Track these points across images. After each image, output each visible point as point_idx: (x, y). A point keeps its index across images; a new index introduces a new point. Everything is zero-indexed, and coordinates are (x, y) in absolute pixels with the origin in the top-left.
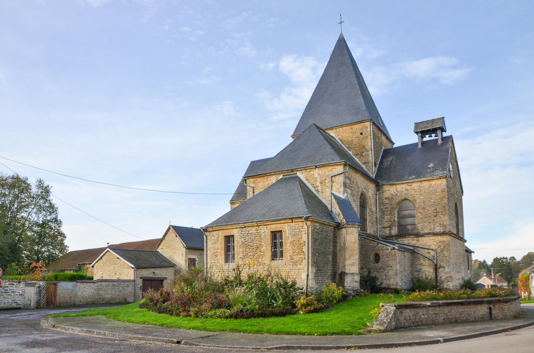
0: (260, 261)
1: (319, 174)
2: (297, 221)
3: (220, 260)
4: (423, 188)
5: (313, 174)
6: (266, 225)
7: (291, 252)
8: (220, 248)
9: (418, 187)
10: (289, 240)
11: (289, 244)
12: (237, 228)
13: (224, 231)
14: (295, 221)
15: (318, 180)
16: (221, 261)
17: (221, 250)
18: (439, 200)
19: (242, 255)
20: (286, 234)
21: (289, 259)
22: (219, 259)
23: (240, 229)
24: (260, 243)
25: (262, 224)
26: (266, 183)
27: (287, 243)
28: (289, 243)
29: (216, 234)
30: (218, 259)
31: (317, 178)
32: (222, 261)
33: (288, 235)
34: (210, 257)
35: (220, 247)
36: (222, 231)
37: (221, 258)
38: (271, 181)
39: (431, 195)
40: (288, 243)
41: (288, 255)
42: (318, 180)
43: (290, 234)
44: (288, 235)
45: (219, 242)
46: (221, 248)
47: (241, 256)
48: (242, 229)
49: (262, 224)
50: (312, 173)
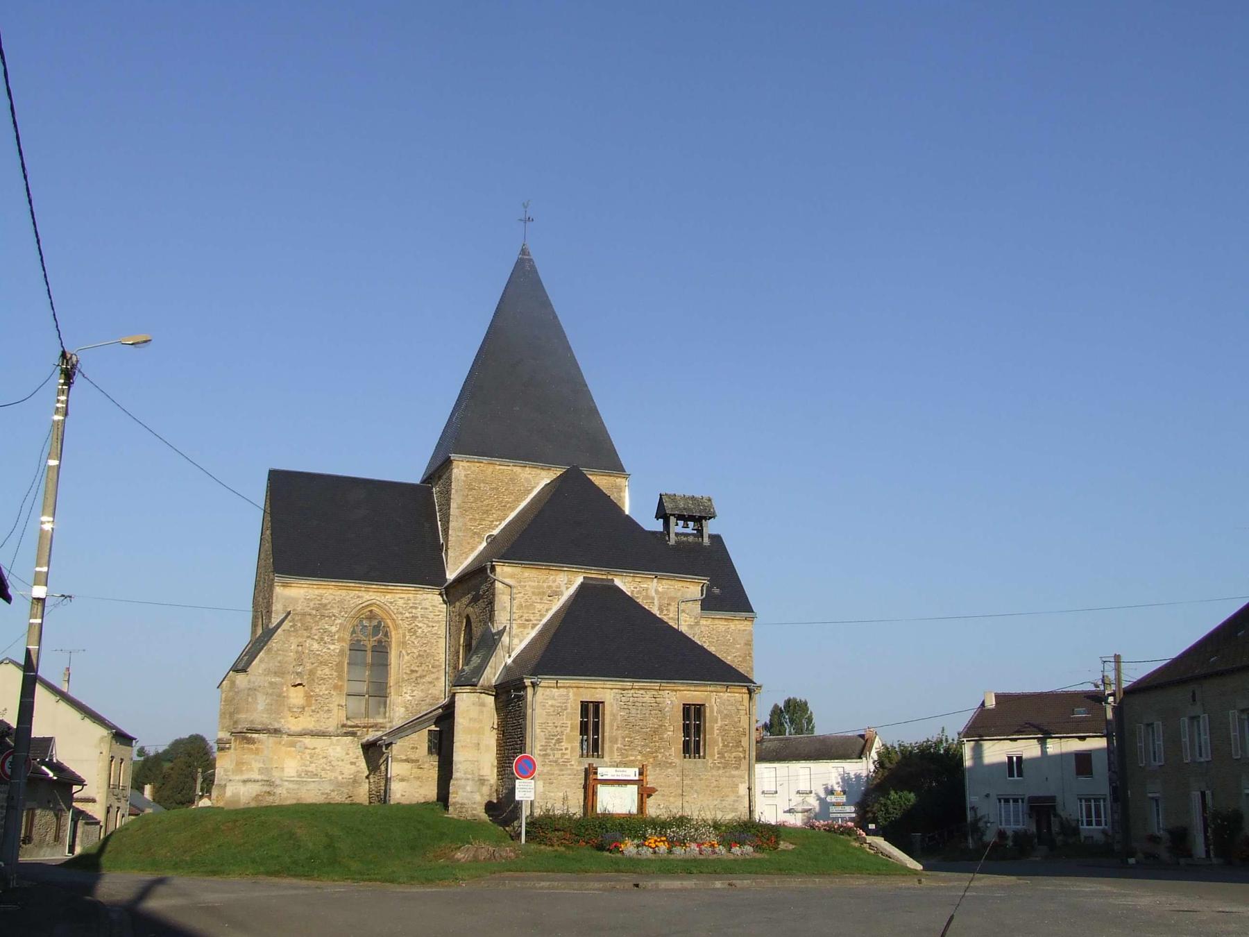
0: (660, 756)
1: (657, 591)
2: (736, 690)
3: (568, 752)
4: (715, 632)
5: (647, 589)
6: (676, 691)
7: (721, 745)
8: (569, 725)
9: (707, 628)
10: (717, 723)
11: (718, 731)
12: (612, 689)
13: (581, 690)
14: (732, 690)
15: (656, 602)
16: (571, 752)
17: (571, 731)
18: (740, 659)
19: (621, 744)
20: (712, 711)
21: (716, 758)
22: (566, 749)
23: (620, 691)
24: (660, 723)
25: (668, 688)
26: (545, 585)
27: (713, 728)
28: (718, 729)
29: (560, 696)
30: (563, 748)
31: (653, 599)
32: (575, 754)
33: (715, 714)
34: (543, 744)
35: (569, 723)
36: (575, 689)
37: (572, 748)
38: (556, 584)
39: (727, 648)
40: (716, 728)
41: (716, 751)
42: (656, 602)
43: (719, 712)
44: (715, 714)
45: (567, 714)
46: (571, 725)
47: (619, 745)
48: (623, 692)
49: (668, 688)
50: (645, 586)
